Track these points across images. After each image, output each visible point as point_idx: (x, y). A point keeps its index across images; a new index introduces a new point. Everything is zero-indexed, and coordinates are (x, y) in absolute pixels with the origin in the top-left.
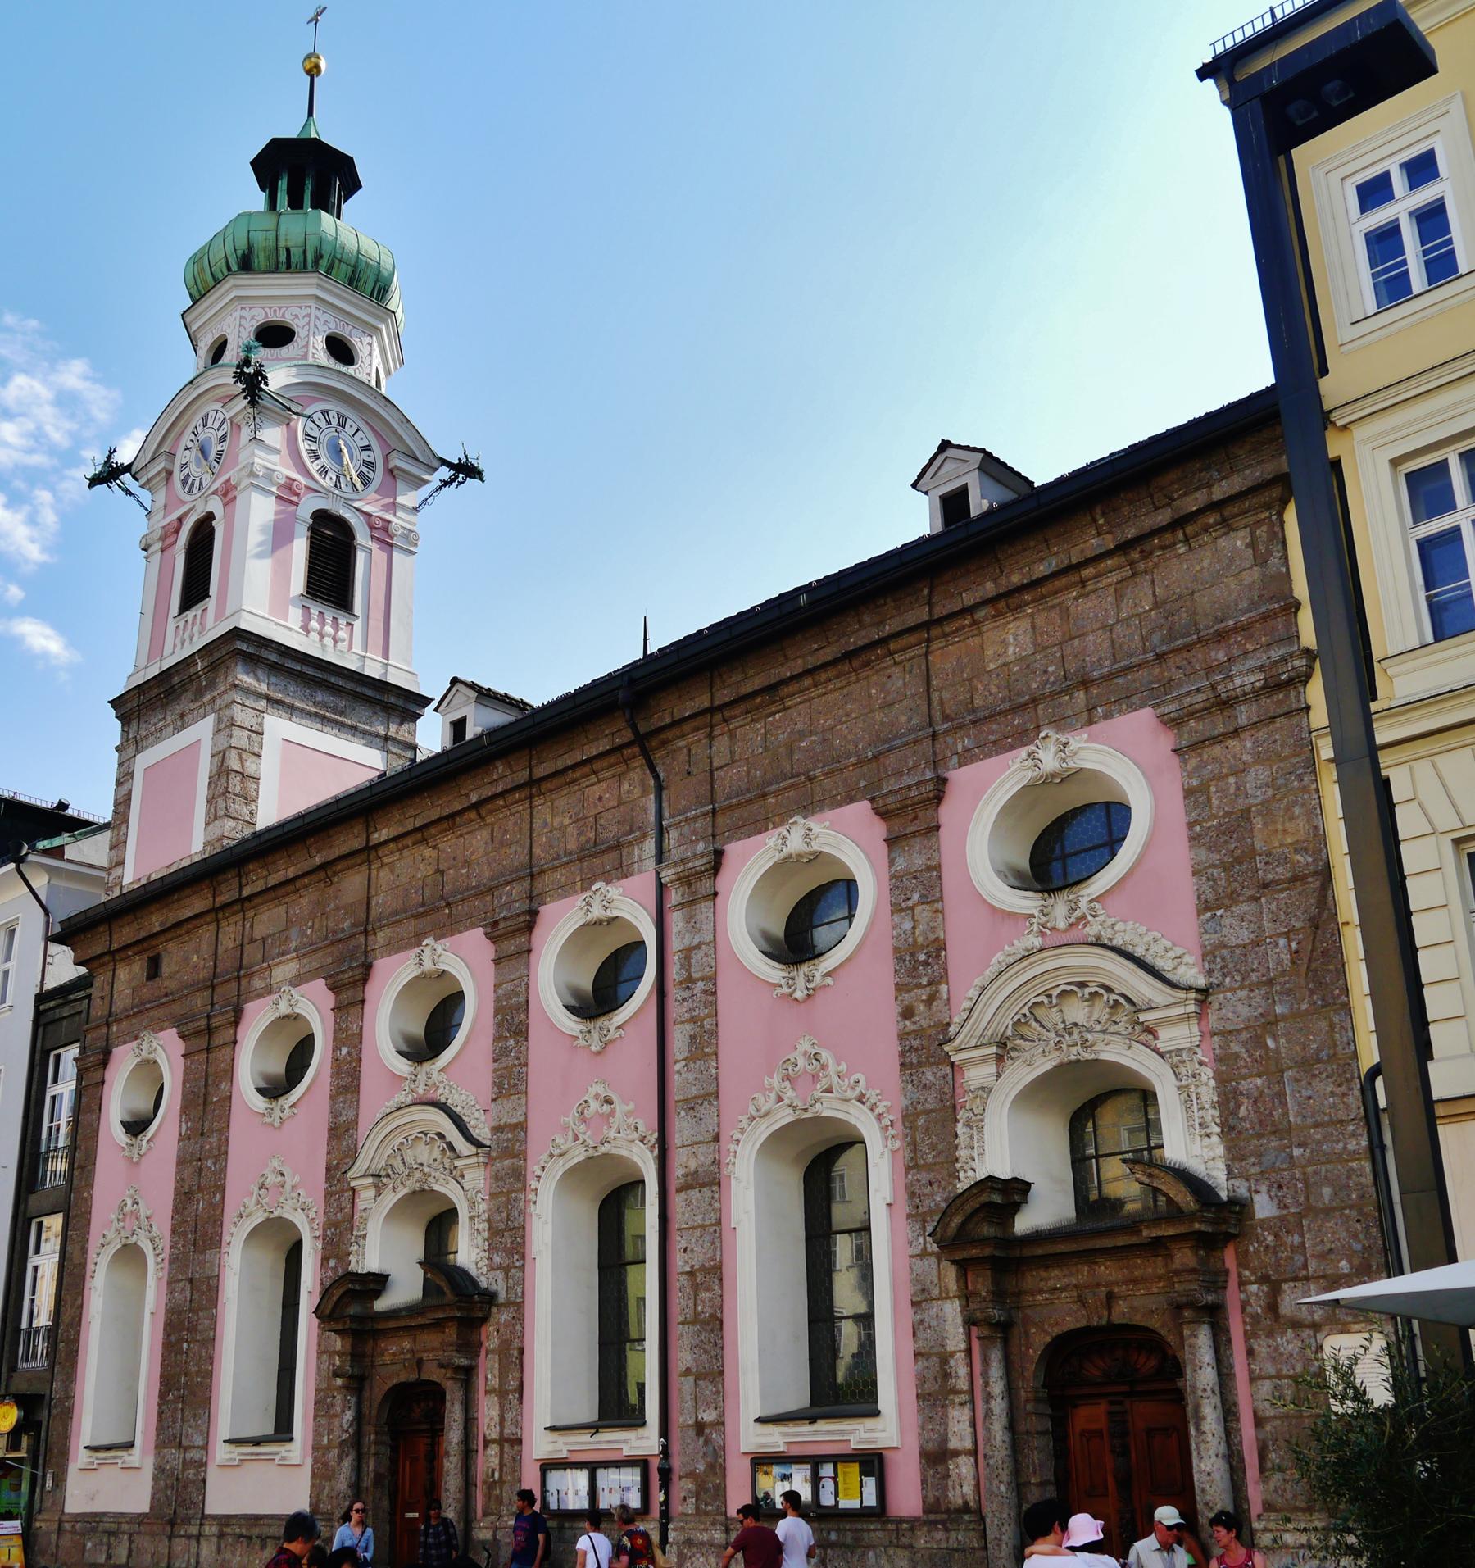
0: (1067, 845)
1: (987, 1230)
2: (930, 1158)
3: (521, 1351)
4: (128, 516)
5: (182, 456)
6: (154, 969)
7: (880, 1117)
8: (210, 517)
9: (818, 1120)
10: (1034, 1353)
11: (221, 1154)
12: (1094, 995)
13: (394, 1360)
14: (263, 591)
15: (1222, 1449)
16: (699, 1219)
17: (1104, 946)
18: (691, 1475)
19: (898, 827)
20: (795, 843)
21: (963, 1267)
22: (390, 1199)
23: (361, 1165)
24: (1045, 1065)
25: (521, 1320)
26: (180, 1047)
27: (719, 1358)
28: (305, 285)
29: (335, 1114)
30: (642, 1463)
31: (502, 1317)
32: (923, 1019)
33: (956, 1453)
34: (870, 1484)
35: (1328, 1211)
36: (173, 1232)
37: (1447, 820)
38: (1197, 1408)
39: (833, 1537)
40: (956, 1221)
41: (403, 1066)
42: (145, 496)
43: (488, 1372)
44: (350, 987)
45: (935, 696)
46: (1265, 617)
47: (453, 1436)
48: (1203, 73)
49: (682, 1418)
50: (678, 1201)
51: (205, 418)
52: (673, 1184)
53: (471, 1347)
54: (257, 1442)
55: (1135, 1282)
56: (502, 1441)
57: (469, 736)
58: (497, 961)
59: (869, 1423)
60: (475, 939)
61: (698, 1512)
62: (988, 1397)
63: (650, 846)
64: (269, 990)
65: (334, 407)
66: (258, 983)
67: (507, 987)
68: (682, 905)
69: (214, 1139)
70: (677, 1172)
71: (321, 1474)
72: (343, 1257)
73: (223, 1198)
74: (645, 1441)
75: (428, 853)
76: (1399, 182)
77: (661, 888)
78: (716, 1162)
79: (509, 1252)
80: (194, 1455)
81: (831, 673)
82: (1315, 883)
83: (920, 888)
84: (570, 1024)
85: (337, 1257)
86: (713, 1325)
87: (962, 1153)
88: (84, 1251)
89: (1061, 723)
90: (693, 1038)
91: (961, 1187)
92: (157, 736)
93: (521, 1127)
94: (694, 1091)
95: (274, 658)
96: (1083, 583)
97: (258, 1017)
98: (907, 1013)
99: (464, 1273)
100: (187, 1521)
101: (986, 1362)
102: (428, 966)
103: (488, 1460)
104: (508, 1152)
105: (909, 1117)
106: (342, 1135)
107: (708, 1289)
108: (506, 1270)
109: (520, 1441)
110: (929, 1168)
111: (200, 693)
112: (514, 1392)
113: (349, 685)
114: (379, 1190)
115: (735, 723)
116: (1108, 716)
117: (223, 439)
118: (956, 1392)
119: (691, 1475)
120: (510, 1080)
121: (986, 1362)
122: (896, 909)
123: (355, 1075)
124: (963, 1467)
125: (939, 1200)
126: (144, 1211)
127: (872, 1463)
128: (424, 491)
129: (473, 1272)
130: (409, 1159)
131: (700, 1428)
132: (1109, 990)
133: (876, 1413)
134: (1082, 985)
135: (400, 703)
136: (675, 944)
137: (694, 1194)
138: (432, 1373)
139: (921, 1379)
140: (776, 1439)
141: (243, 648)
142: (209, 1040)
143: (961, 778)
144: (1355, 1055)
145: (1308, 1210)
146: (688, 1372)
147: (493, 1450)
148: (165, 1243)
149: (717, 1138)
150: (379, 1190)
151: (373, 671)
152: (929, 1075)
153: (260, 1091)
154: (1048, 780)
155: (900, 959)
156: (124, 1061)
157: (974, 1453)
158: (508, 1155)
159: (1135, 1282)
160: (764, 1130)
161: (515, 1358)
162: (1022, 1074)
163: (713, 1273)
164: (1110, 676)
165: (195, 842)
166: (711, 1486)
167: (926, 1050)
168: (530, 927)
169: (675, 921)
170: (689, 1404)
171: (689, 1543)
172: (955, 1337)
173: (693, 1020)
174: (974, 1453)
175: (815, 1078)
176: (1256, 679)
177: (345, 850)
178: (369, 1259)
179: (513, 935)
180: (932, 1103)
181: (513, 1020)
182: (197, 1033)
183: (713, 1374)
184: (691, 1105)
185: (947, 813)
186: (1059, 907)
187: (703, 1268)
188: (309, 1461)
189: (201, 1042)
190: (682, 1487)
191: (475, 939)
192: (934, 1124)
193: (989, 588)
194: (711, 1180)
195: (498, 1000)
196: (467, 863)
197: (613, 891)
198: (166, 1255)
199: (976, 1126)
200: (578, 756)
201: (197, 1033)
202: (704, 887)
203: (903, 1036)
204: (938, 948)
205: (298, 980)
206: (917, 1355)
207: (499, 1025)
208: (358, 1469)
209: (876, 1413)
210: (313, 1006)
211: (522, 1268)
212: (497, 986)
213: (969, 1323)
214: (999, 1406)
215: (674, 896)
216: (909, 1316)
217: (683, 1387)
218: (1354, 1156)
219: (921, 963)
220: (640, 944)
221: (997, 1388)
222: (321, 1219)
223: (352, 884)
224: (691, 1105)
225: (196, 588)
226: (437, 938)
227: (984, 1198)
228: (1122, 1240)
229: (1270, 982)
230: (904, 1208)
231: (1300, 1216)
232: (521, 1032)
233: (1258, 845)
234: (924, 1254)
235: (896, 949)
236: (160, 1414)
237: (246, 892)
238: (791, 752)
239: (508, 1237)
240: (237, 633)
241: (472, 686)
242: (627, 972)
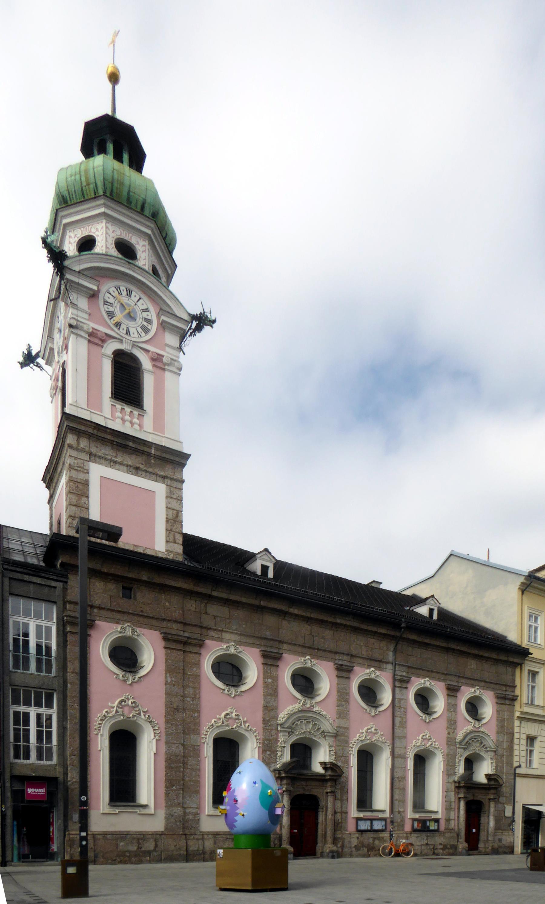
34: (436, 824)
36: (167, 722)
66: (212, 633)
67: (342, 686)
139: (446, 806)
173: (400, 717)
195: (338, 688)
198: (163, 730)
230: (445, 772)
236: (167, 795)
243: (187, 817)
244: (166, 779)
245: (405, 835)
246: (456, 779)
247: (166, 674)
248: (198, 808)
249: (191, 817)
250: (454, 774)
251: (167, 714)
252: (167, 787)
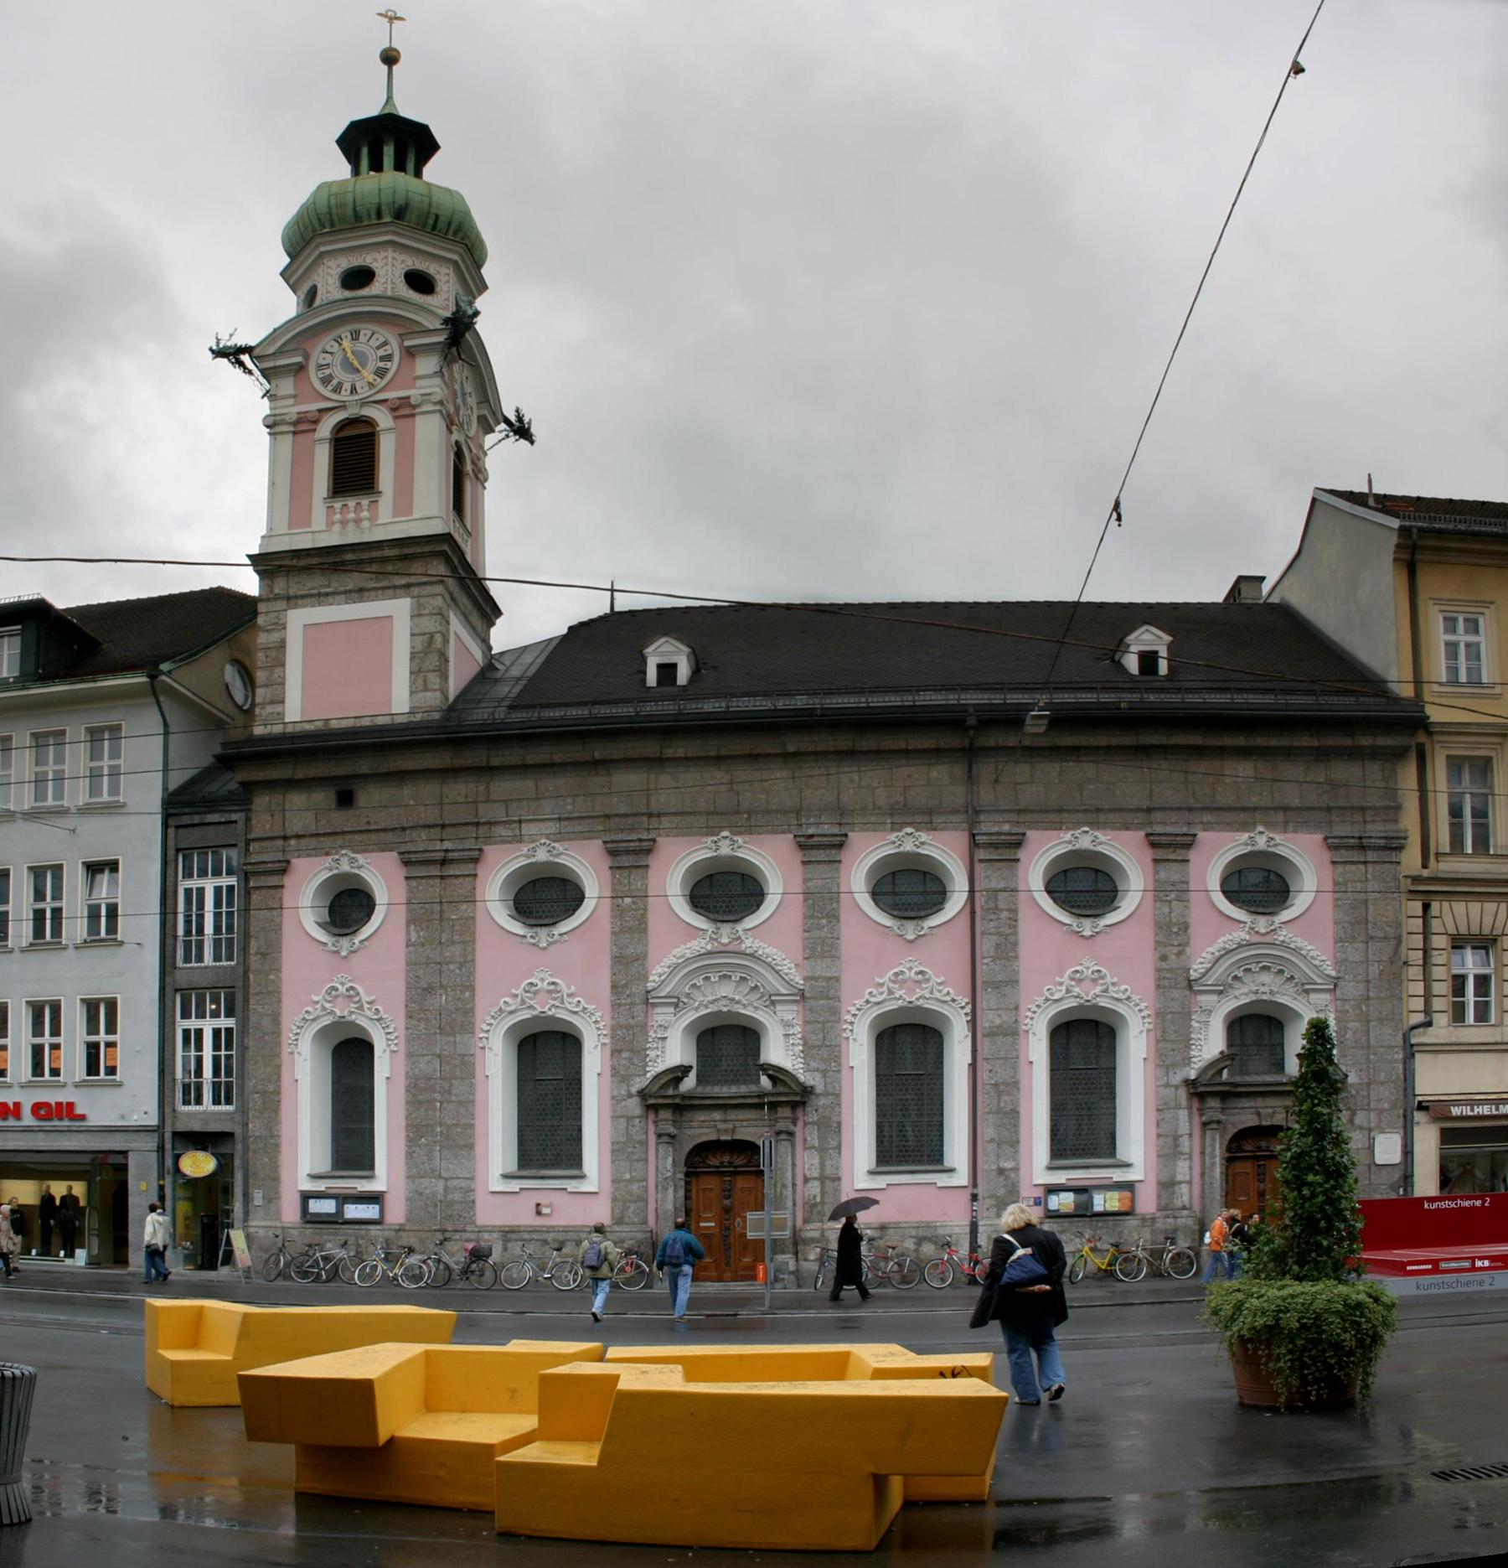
2: (1173, 1037)
16: (1002, 1054)
19: (1162, 854)
25: (839, 1105)
27: (1017, 1132)
31: (822, 1101)
36: (409, 1016)
56: (822, 1179)
73: (473, 997)
85: (631, 1050)
98: (1163, 958)
105: (1160, 1015)
107: (1009, 1094)
108: (824, 1073)
109: (839, 1179)
124: (1185, 1188)
131: (1001, 1171)
146: (992, 1140)
149: (1017, 1008)
158: (819, 1002)
198: (402, 1032)
203: (1158, 970)
204: (1185, 927)
206: (1159, 1136)
211: (839, 1071)
224: (996, 985)
235: (1156, 923)
236: (410, 1155)
243: (450, 1197)
244: (408, 1126)
246: (1193, 1075)
247: (408, 926)
248: (472, 1179)
249: (457, 1196)
250: (1187, 1061)
251: (410, 1000)
252: (409, 1139)
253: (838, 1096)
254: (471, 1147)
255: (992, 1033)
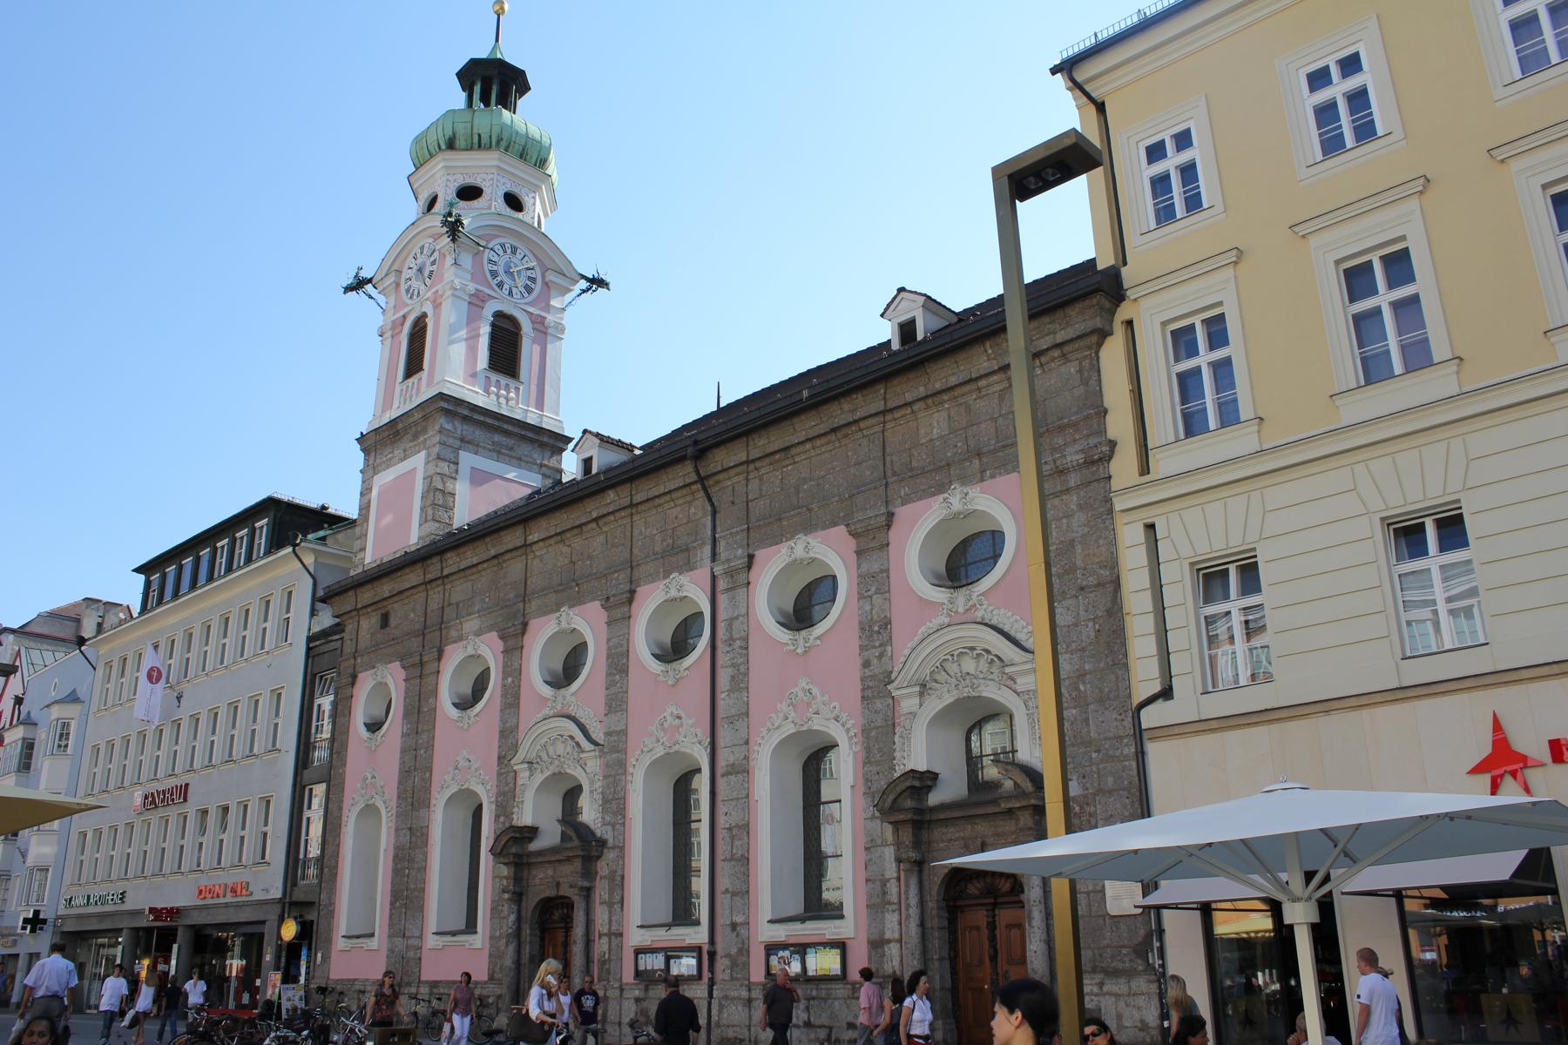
0: (964, 561)
1: (909, 803)
2: (878, 757)
3: (623, 877)
4: (369, 312)
5: (406, 274)
6: (385, 621)
7: (848, 731)
8: (424, 315)
9: (810, 731)
10: (938, 880)
11: (430, 746)
12: (979, 655)
13: (542, 883)
14: (458, 367)
15: (1044, 936)
17: (986, 625)
18: (728, 956)
20: (799, 552)
21: (896, 825)
22: (539, 778)
23: (521, 755)
24: (949, 699)
26: (402, 674)
28: (491, 159)
29: (504, 721)
30: (697, 950)
31: (609, 855)
32: (876, 668)
33: (889, 941)
35: (1110, 792)
37: (1186, 552)
38: (1030, 912)
39: (814, 993)
40: (891, 797)
41: (547, 691)
42: (381, 299)
43: (601, 891)
44: (514, 636)
45: (888, 459)
46: (1087, 418)
47: (578, 931)
48: (1055, 71)
49: (723, 920)
50: (721, 783)
51: (422, 248)
52: (719, 772)
53: (589, 873)
54: (454, 934)
55: (998, 835)
56: (610, 934)
57: (594, 471)
58: (609, 623)
59: (837, 922)
60: (594, 608)
61: (732, 979)
62: (908, 906)
63: (708, 549)
64: (461, 638)
65: (509, 241)
67: (615, 640)
68: (728, 590)
69: (425, 736)
70: (722, 764)
71: (495, 956)
72: (509, 816)
74: (699, 935)
75: (565, 549)
76: (1170, 147)
77: (714, 578)
78: (747, 758)
79: (615, 814)
80: (412, 942)
81: (823, 440)
82: (1110, 588)
83: (875, 583)
84: (656, 666)
86: (744, 861)
87: (897, 754)
88: (341, 808)
89: (965, 480)
90: (733, 677)
91: (896, 775)
92: (388, 464)
93: (624, 732)
94: (733, 712)
95: (466, 412)
96: (979, 390)
97: (454, 657)
98: (866, 664)
99: (587, 827)
100: (409, 984)
101: (907, 886)
102: (564, 625)
103: (601, 946)
104: (615, 749)
105: (865, 731)
106: (508, 737)
108: (613, 826)
110: (878, 763)
111: (416, 436)
112: (618, 902)
113: (516, 430)
114: (532, 771)
115: (763, 471)
116: (992, 477)
117: (433, 263)
118: (890, 903)
119: (728, 956)
120: (616, 702)
121: (907, 886)
122: (861, 597)
123: (517, 696)
124: (893, 950)
125: (883, 784)
126: (379, 782)
127: (841, 946)
128: (569, 297)
129: (592, 827)
130: (551, 752)
131: (734, 926)
132: (988, 652)
133: (842, 917)
134: (972, 649)
135: (551, 441)
136: (722, 615)
137: (732, 778)
138: (565, 891)
139: (870, 896)
140: (780, 933)
141: (448, 406)
142: (421, 672)
143: (903, 512)
144: (1130, 696)
145: (1099, 791)
146: (727, 891)
147: (605, 940)
148: (394, 803)
149: (747, 743)
150: (532, 771)
151: (532, 420)
152: (879, 704)
153: (455, 705)
154: (956, 516)
155: (862, 629)
156: (366, 684)
157: (900, 941)
158: (614, 750)
159: (998, 835)
160: (776, 738)
161: (618, 882)
162: (935, 704)
163: (744, 829)
164: (994, 451)
165: (414, 537)
166: (740, 960)
167: (876, 685)
168: (630, 601)
169: (722, 600)
170: (727, 912)
171: (726, 997)
172: (891, 870)
173: (733, 665)
174: (900, 941)
175: (809, 705)
176: (1080, 458)
177: (510, 546)
178: (525, 816)
179: (620, 605)
180: (879, 723)
181: (619, 662)
182: (413, 666)
183: (743, 893)
184: (731, 720)
185: (894, 535)
186: (961, 596)
187: (737, 826)
188: (488, 946)
189: (417, 671)
190: (722, 964)
191: (594, 608)
192: (880, 735)
193: (922, 391)
194: (742, 769)
196: (590, 557)
197: (684, 579)
199: (907, 737)
200: (662, 490)
201: (413, 666)
202: (742, 578)
204: (886, 623)
205: (479, 633)
206: (867, 880)
207: (609, 666)
208: (519, 952)
209: (842, 917)
210: (489, 649)
211: (624, 824)
212: (609, 640)
213: (899, 861)
214: (914, 911)
215: (722, 584)
216: (863, 856)
217: (723, 901)
218: (1127, 758)
219: (876, 631)
220: (699, 615)
221: (914, 901)
222: (495, 790)
223: (515, 568)
224: (731, 720)
225: (414, 364)
226: (571, 607)
227: (908, 784)
228: (990, 810)
229: (1083, 650)
230: (861, 788)
231: (1095, 795)
232: (624, 671)
233: (1079, 563)
234: (873, 818)
237: (446, 572)
238: (798, 492)
239: (615, 804)
240: (441, 396)
241: (597, 435)
242: (693, 632)
245: (744, 994)
249: (411, 954)
253: (622, 849)
254: (421, 908)
255: (733, 770)
